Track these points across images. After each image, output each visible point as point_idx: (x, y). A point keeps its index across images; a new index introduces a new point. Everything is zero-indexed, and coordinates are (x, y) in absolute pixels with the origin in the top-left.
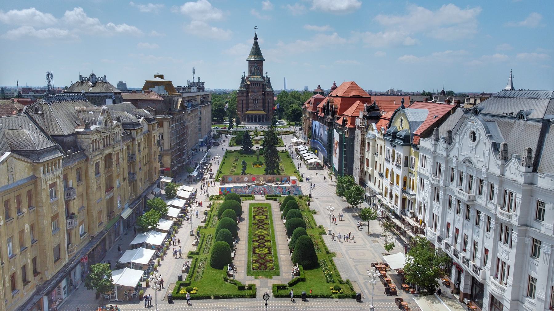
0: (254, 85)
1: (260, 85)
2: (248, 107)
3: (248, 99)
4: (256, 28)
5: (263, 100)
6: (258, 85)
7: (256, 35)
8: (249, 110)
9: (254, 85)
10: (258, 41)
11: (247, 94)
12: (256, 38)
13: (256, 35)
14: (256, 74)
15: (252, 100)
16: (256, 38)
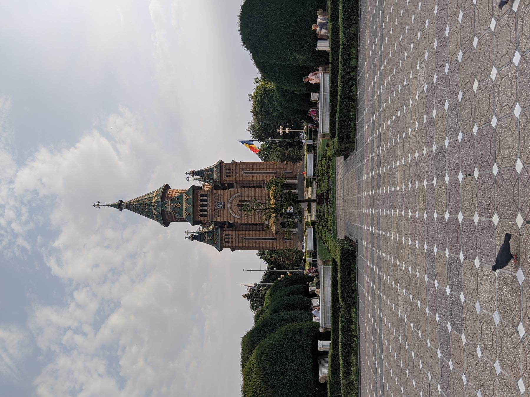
0: (206, 210)
1: (206, 195)
2: (262, 224)
3: (243, 224)
4: (98, 205)
5: (243, 187)
6: (206, 200)
7: (112, 206)
8: (266, 222)
9: (206, 210)
10: (125, 201)
11: (231, 226)
12: (120, 206)
13: (112, 206)
14: (178, 205)
15: (241, 215)
16: (120, 206)
